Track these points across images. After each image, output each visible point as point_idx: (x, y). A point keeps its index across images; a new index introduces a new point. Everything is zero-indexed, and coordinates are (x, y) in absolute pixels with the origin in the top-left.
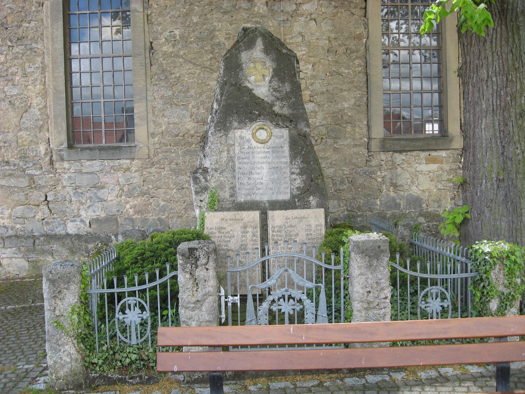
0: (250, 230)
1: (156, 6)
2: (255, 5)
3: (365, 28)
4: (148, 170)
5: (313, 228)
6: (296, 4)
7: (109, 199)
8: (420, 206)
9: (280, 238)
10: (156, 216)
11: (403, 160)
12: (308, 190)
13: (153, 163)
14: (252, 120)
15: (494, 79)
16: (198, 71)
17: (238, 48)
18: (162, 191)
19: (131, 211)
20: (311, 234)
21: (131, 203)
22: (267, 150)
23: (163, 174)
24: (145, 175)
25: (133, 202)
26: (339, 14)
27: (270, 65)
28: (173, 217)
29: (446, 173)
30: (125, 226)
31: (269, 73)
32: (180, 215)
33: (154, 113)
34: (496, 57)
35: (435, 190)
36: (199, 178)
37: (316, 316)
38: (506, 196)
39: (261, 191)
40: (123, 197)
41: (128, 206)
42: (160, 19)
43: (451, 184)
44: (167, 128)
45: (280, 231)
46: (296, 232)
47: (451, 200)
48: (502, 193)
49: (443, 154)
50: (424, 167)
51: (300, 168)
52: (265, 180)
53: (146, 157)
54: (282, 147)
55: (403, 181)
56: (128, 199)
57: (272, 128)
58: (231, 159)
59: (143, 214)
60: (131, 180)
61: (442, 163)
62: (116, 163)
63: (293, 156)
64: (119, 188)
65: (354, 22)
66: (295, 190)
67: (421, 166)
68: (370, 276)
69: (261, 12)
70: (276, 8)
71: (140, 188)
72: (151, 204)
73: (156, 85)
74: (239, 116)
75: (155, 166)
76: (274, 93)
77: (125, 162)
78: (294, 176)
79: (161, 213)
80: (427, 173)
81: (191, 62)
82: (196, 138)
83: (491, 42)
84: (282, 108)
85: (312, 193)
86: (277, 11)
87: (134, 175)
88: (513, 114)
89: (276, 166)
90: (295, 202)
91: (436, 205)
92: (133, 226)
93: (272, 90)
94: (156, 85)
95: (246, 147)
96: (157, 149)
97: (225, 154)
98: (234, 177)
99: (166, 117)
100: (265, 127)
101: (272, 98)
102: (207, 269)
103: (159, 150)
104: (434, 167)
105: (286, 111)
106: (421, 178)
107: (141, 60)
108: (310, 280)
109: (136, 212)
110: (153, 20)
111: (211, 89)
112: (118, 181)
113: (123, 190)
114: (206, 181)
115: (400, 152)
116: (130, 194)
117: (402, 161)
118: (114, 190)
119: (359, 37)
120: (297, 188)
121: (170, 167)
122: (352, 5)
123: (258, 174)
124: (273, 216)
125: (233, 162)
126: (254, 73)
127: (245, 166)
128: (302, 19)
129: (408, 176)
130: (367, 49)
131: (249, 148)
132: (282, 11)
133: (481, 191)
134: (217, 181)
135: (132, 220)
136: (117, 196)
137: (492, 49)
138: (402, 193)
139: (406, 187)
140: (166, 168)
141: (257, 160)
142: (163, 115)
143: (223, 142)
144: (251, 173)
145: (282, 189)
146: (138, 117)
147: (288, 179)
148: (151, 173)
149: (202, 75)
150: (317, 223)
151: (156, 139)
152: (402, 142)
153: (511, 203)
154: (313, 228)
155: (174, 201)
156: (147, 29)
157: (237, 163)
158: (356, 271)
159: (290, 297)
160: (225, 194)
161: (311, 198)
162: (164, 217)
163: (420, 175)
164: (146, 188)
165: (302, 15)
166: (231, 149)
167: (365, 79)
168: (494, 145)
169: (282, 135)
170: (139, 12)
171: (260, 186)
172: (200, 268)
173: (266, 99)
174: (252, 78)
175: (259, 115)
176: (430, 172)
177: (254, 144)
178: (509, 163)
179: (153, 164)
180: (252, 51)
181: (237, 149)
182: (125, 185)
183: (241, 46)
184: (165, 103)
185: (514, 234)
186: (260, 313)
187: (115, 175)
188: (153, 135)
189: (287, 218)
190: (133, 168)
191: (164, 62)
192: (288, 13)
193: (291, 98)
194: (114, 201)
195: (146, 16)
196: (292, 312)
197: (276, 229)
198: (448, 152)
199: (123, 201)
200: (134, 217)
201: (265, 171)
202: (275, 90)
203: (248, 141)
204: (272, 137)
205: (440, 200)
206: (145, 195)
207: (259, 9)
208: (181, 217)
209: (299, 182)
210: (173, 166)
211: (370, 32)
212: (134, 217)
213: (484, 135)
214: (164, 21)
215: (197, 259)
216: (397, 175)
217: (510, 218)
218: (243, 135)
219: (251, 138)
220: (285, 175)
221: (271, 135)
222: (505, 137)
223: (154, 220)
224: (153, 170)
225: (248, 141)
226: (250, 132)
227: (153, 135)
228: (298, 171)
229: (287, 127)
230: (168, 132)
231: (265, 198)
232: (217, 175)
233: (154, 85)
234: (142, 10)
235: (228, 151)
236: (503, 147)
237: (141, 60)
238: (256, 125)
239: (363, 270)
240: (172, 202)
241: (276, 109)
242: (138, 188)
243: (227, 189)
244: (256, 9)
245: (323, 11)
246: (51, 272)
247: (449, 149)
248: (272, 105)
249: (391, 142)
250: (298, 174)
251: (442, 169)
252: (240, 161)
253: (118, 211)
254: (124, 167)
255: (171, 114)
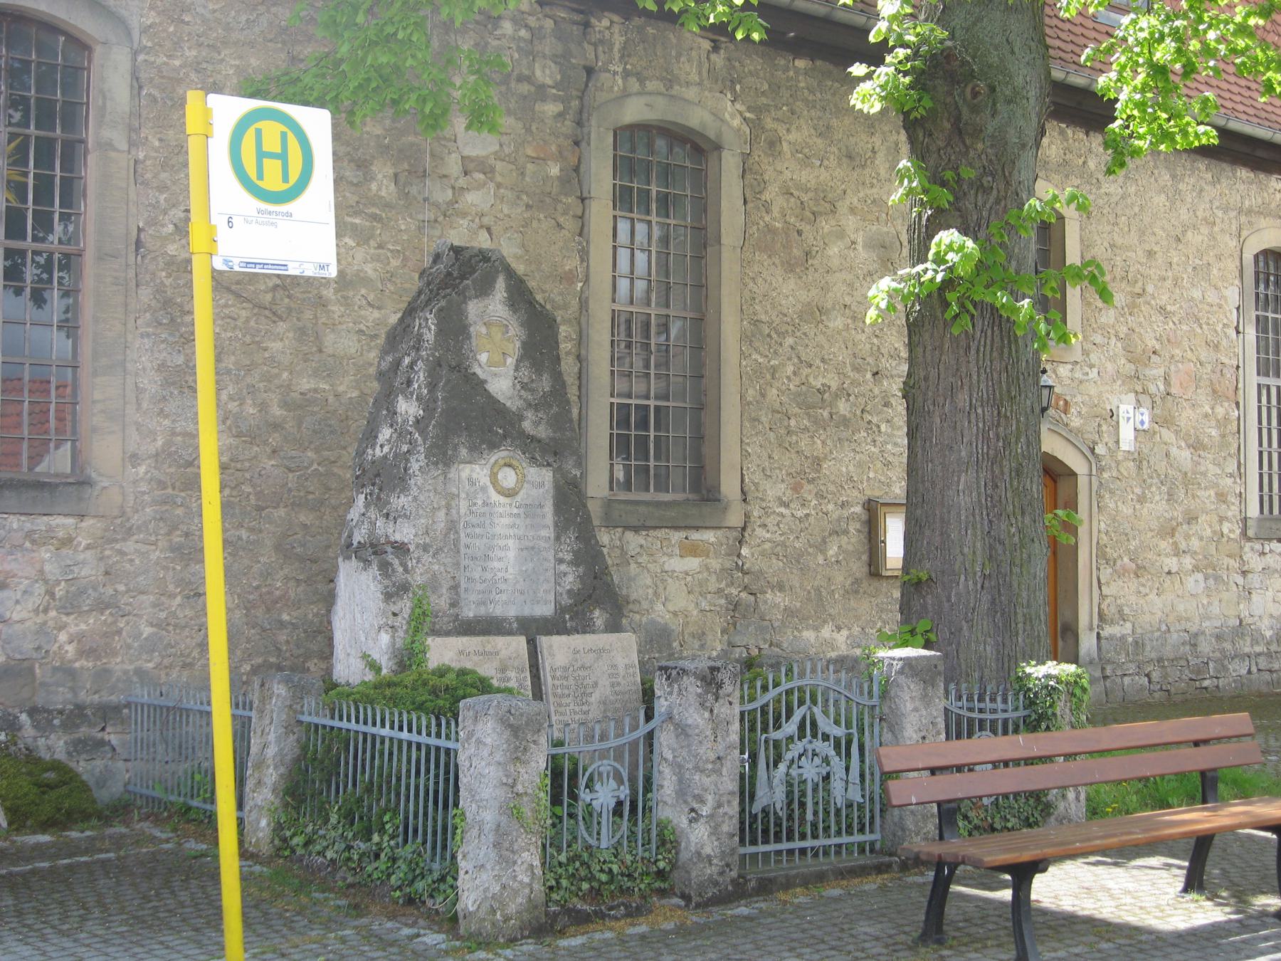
0: (512, 674)
1: (157, 144)
2: (373, 179)
3: (582, 261)
4: (118, 546)
5: (621, 671)
6: (453, 188)
7: (16, 617)
8: (670, 645)
9: (566, 692)
10: (131, 662)
11: (641, 546)
12: (590, 597)
13: (130, 528)
14: (493, 446)
15: (980, 411)
16: (244, 313)
17: (463, 292)
18: (148, 599)
19: (70, 649)
20: (619, 684)
21: (73, 629)
22: (515, 511)
23: (154, 557)
24: (109, 557)
25: (77, 625)
26: (535, 224)
27: (516, 331)
28: (170, 667)
29: (713, 578)
30: (53, 688)
31: (514, 348)
32: (189, 660)
33: (139, 404)
34: (983, 376)
35: (695, 613)
36: (391, 564)
37: (847, 782)
38: (993, 602)
39: (504, 597)
40: (53, 613)
41: (63, 637)
42: (164, 175)
43: (723, 601)
44: (168, 443)
45: (566, 678)
46: (594, 679)
47: (722, 633)
48: (986, 598)
49: (710, 536)
50: (678, 564)
51: (573, 552)
52: (511, 573)
53: (116, 512)
54: (541, 506)
55: (641, 592)
56: (64, 618)
57: (524, 465)
58: (452, 526)
59: (98, 658)
60: (76, 569)
61: (708, 556)
62: (42, 523)
63: (561, 528)
64: (42, 591)
65: (561, 244)
66: (565, 596)
67: (672, 561)
68: (924, 713)
69: (383, 194)
70: (414, 190)
71: (95, 589)
72: (119, 632)
73: (148, 335)
74: (470, 436)
75: (136, 537)
76: (523, 392)
77: (63, 523)
78: (563, 567)
79: (144, 657)
80: (681, 576)
81: (229, 289)
82: (233, 474)
83: (978, 350)
84: (536, 424)
85: (598, 603)
86: (415, 198)
87: (81, 557)
88: (1006, 470)
89: (531, 544)
90: (565, 622)
91: (697, 644)
92: (73, 689)
93: (518, 387)
94: (148, 335)
95: (480, 502)
96: (144, 493)
97: (441, 514)
98: (458, 564)
99: (166, 417)
100: (514, 463)
101: (520, 403)
102: (731, 703)
103: (146, 497)
104: (693, 563)
105: (543, 432)
106: (673, 586)
107: (116, 271)
108: (837, 722)
109: (82, 653)
110: (148, 176)
111: (272, 358)
112: (41, 572)
113: (52, 595)
114: (406, 570)
115: (636, 529)
116: (70, 606)
117: (638, 550)
118: (32, 594)
119: (569, 278)
120: (569, 592)
121: (170, 541)
122: (559, 207)
123: (500, 559)
124: (551, 646)
125: (457, 532)
126: (488, 347)
127: (478, 542)
128: (464, 222)
129: (649, 581)
130: (584, 304)
131: (485, 504)
132: (425, 200)
133: (957, 594)
134: (427, 572)
135: (71, 673)
136: (36, 611)
137: (978, 361)
138: (637, 617)
139: (645, 605)
140: (160, 544)
141: (498, 530)
142: (162, 410)
143: (439, 489)
144: (487, 557)
145: (541, 594)
146: (103, 411)
147: (550, 573)
148: (126, 554)
149: (252, 323)
150: (626, 661)
151: (142, 469)
152: (642, 509)
153: (1002, 615)
154: (621, 671)
155: (176, 626)
156: (133, 196)
157: (462, 535)
158: (908, 704)
159: (815, 754)
160: (440, 601)
161: (597, 613)
162: (151, 665)
163: (670, 580)
164: (111, 592)
165: (464, 215)
166: (453, 503)
167: (576, 370)
168: (978, 518)
169: (540, 480)
170: (119, 151)
171: (503, 586)
172: (721, 701)
173: (508, 404)
174: (483, 357)
175: (505, 437)
176: (687, 574)
177: (495, 497)
178: (1000, 549)
179: (129, 532)
180: (486, 301)
181: (463, 505)
182: (58, 582)
183: (467, 287)
184: (167, 383)
185: (1006, 665)
186: (776, 781)
187: (36, 555)
188: (134, 459)
189: (576, 652)
190: (79, 539)
191: (168, 282)
192: (437, 205)
193: (551, 406)
194: (28, 624)
195: (132, 163)
196: (816, 780)
197: (558, 674)
198: (719, 533)
199: (51, 623)
200: (77, 665)
201: (511, 554)
202: (524, 386)
203: (484, 489)
204: (525, 485)
205: (704, 633)
206: (107, 607)
207: (380, 189)
208: (191, 665)
209: (570, 581)
210: (177, 539)
211: (592, 269)
212: (77, 665)
213: (964, 501)
214: (174, 183)
215: (720, 686)
216: (630, 579)
217: (1000, 639)
218: (475, 476)
219: (489, 484)
220: (546, 565)
221: (522, 480)
222: (994, 506)
223: (126, 672)
224: (130, 546)
225: (484, 489)
226: (486, 471)
227: (134, 459)
228: (568, 557)
229: (549, 465)
230: (170, 455)
231: (512, 612)
232: (427, 558)
233: (142, 336)
234: (125, 147)
235: (448, 507)
236: (990, 522)
237: (116, 271)
238: (501, 455)
239: (917, 703)
240: (171, 628)
241: (527, 425)
242: (90, 591)
243: (444, 591)
244: (374, 186)
245: (506, 211)
246: (509, 712)
247: (720, 528)
248: (521, 418)
249: (622, 506)
250: (570, 563)
251: (708, 569)
252: (469, 531)
253: (39, 648)
254: (61, 534)
255: (180, 411)
